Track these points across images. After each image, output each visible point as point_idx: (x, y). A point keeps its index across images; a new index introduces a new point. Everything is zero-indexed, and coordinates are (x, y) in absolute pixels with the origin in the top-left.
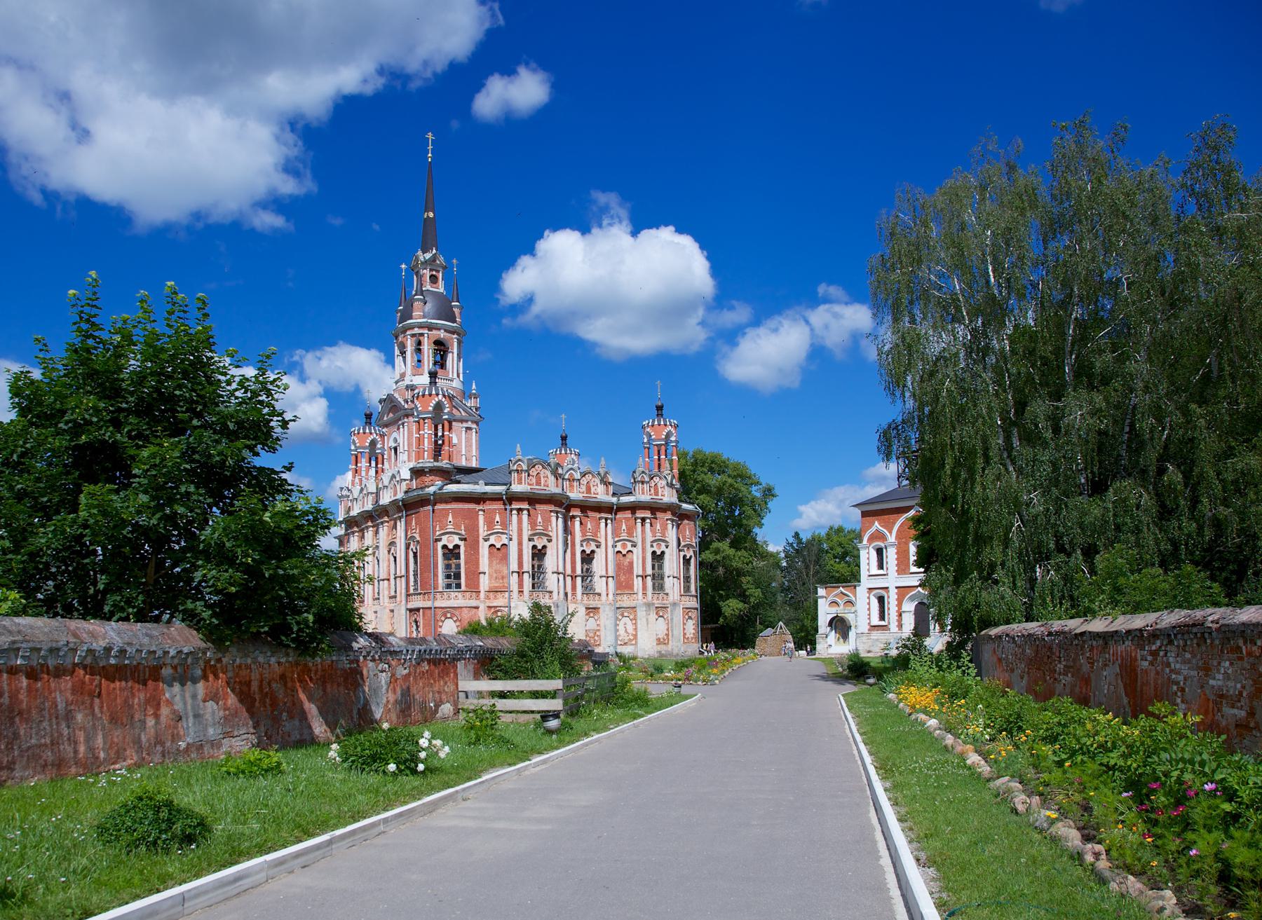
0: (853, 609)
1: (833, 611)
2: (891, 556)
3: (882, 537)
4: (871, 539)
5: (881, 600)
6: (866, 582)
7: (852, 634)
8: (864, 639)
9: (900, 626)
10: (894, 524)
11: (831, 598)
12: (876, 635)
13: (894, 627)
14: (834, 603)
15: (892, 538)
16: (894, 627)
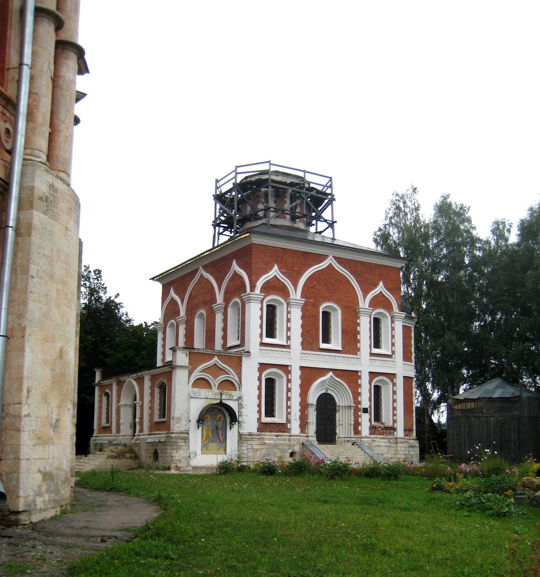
0: (235, 394)
1: (208, 396)
2: (291, 320)
3: (283, 291)
4: (268, 288)
5: (270, 384)
6: (256, 355)
7: (232, 435)
8: (255, 444)
9: (303, 425)
10: (300, 275)
11: (196, 374)
12: (270, 438)
13: (295, 427)
14: (201, 383)
15: (296, 295)
16: (295, 427)
